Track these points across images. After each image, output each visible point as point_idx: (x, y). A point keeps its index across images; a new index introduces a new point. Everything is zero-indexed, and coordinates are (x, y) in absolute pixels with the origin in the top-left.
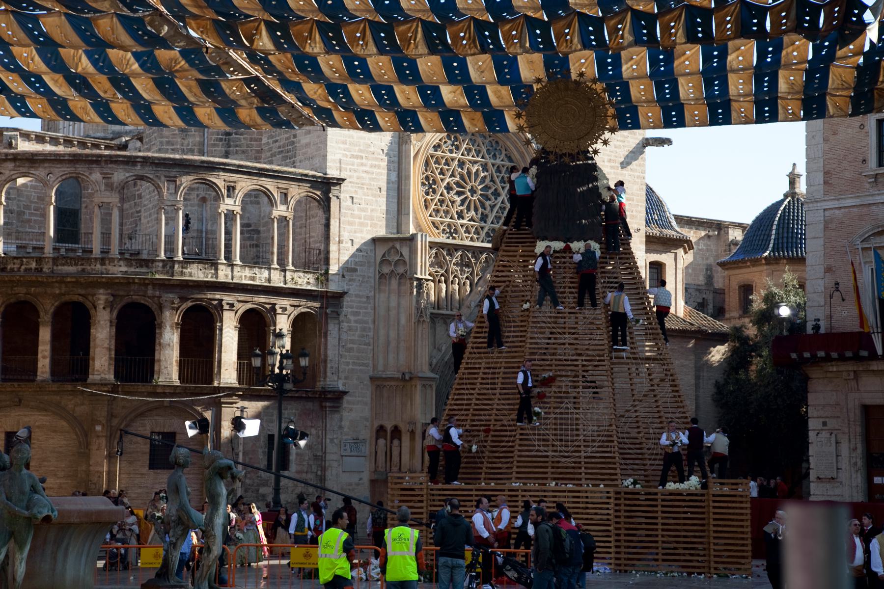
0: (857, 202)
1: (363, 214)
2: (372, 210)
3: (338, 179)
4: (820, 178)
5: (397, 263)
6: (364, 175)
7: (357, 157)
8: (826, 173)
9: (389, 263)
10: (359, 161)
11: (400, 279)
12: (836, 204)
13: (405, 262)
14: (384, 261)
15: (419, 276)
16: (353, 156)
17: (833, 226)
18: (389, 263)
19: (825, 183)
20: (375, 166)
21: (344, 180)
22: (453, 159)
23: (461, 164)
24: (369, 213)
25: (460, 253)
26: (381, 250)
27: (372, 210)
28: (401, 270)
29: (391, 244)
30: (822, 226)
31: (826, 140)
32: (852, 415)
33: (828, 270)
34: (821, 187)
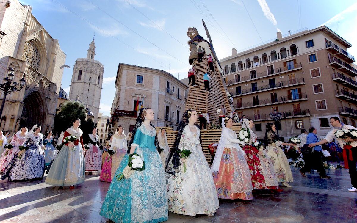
0: (133, 88)
1: (8, 48)
2: (11, 48)
3: (4, 33)
4: (125, 82)
5: (16, 67)
6: (11, 37)
7: (10, 31)
8: (126, 81)
9: (14, 66)
10: (11, 32)
11: (16, 72)
12: (129, 87)
13: (19, 68)
14: (11, 64)
15: (25, 73)
16: (9, 30)
17: (127, 91)
18: (14, 66)
19: (126, 83)
20: (14, 37)
21: (6, 35)
22: (28, 48)
23: (29, 50)
24: (9, 49)
25: (33, 72)
26: (10, 61)
27: (11, 48)
28: (18, 69)
29: (15, 61)
30: (125, 91)
31: (127, 75)
32: (128, 127)
33: (125, 99)
34: (125, 84)
